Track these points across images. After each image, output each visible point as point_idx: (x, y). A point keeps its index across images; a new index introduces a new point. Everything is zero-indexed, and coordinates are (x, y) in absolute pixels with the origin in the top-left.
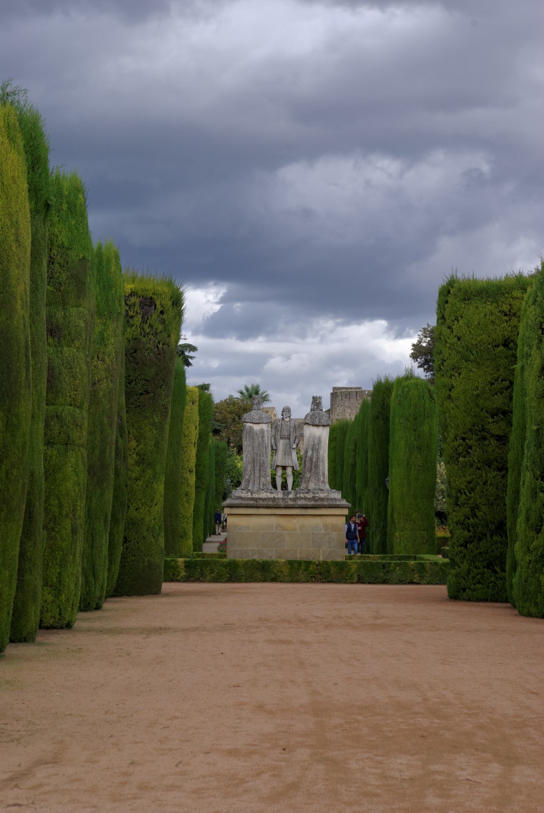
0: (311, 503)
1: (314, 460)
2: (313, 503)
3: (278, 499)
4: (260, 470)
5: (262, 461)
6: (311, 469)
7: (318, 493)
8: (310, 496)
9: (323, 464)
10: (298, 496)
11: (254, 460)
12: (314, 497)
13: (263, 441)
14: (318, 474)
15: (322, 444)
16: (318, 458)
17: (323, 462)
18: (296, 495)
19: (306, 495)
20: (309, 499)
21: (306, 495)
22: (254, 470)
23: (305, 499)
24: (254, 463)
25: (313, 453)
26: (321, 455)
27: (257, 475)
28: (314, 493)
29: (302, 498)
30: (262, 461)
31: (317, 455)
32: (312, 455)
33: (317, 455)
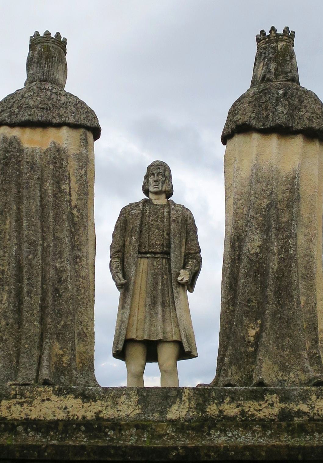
0: (274, 442)
1: (274, 265)
2: (286, 440)
3: (117, 425)
4: (43, 308)
5: (52, 273)
6: (262, 303)
7: (304, 398)
8: (268, 409)
9: (311, 288)
10: (212, 409)
11: (19, 268)
12: (285, 415)
13: (59, 192)
14: (290, 321)
15: (304, 209)
16: (287, 261)
17: (309, 276)
18: (201, 407)
19: (251, 407)
20: (265, 424)
21: (251, 407)
22: (18, 310)
23: (246, 422)
24: (19, 280)
25: (266, 241)
26: (301, 252)
27: (32, 328)
28: (285, 398)
29: (233, 419)
30: (52, 273)
31: (284, 248)
32: (265, 248)
33: (284, 248)
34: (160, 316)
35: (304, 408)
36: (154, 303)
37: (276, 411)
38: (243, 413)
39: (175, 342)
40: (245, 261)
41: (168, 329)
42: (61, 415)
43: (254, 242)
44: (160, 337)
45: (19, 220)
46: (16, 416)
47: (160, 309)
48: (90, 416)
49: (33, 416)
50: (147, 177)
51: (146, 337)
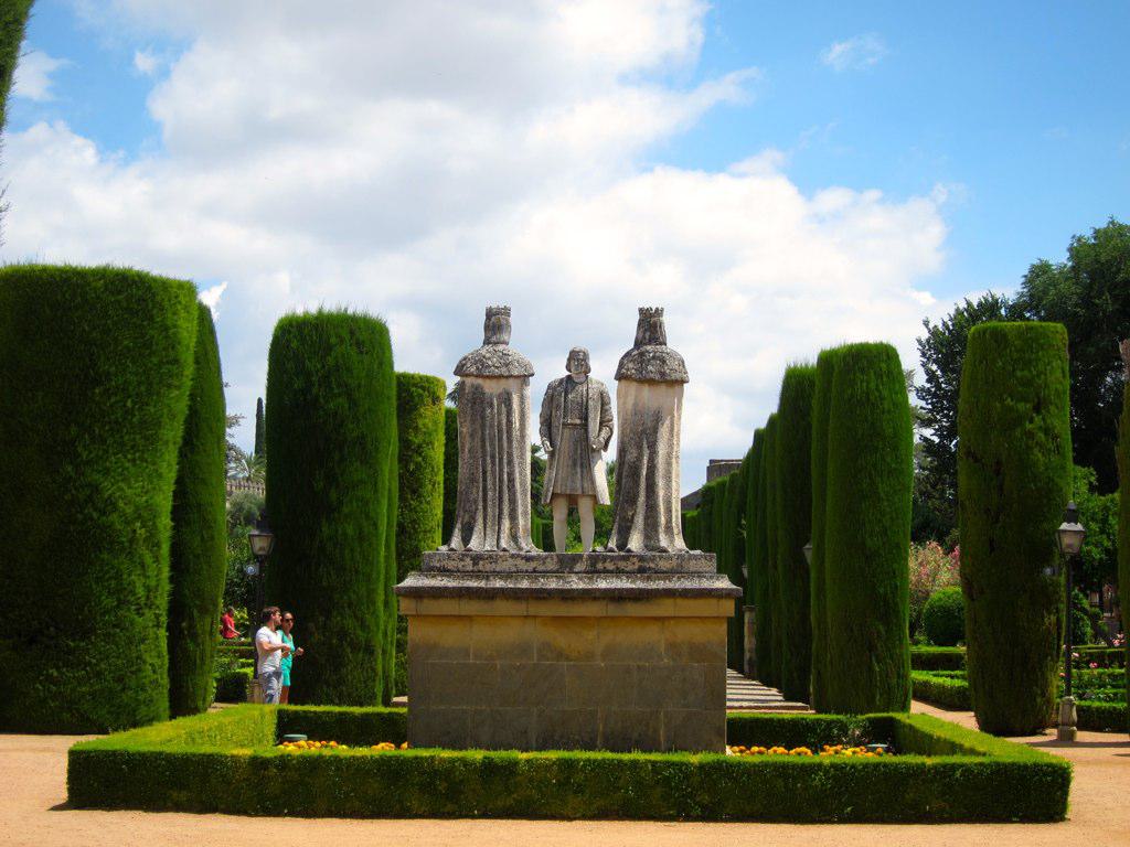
10: (600, 566)
19: (622, 564)
21: (622, 564)
34: (579, 475)
35: (652, 565)
36: (575, 465)
37: (636, 567)
38: (618, 568)
39: (591, 496)
40: (627, 466)
41: (586, 485)
42: (514, 569)
43: (631, 456)
44: (579, 492)
45: (483, 441)
46: (488, 570)
47: (579, 470)
48: (530, 569)
49: (497, 569)
50: (569, 360)
51: (568, 492)
